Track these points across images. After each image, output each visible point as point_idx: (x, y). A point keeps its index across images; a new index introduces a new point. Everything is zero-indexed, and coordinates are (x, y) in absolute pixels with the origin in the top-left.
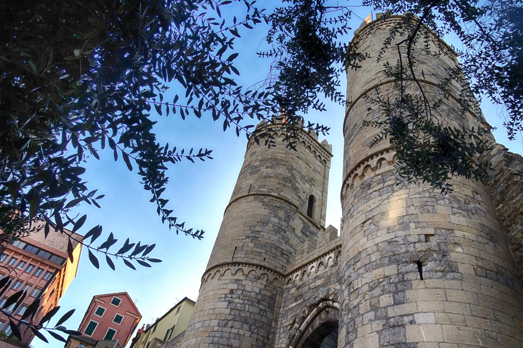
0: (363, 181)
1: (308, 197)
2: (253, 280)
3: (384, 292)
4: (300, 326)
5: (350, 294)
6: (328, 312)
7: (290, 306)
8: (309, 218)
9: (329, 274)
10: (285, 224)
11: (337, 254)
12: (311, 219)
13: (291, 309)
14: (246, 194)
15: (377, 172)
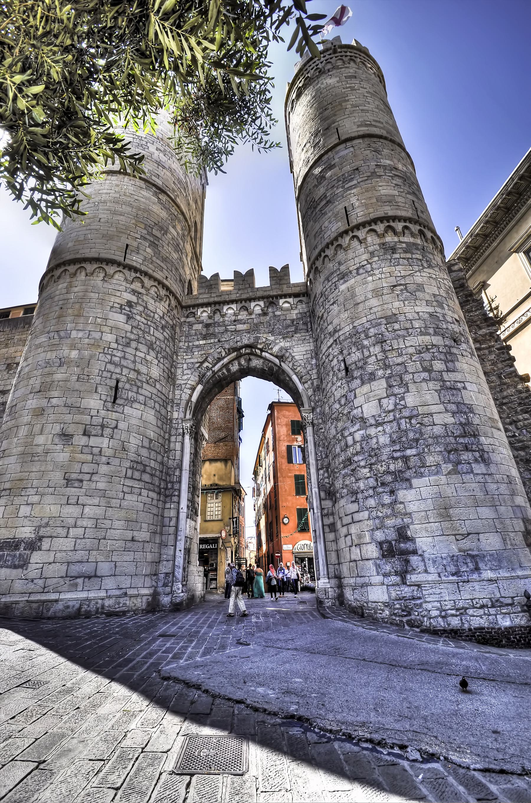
3: (434, 358)
4: (214, 366)
5: (384, 351)
6: (250, 360)
7: (197, 343)
10: (181, 242)
13: (197, 346)
15: (402, 239)
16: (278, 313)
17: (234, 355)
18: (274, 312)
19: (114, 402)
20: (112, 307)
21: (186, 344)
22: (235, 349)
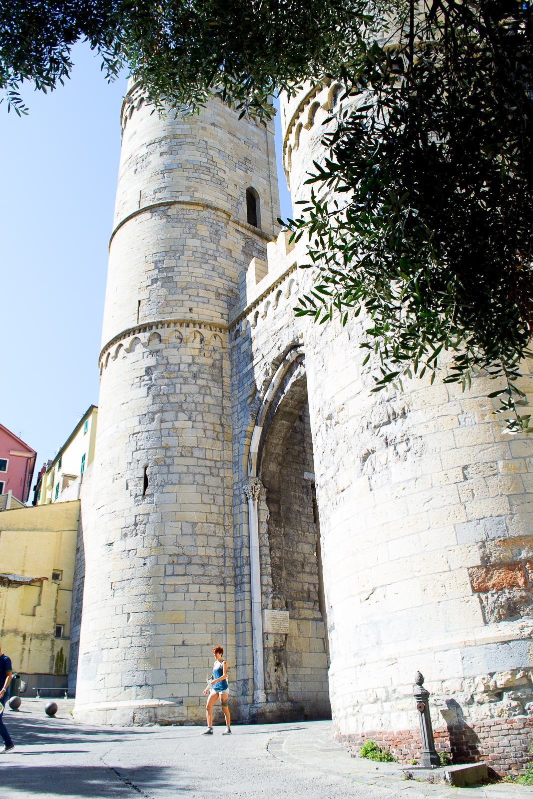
1: (245, 192)
4: (264, 395)
8: (252, 227)
10: (213, 246)
12: (257, 229)
14: (136, 209)
19: (144, 494)
22: (281, 359)
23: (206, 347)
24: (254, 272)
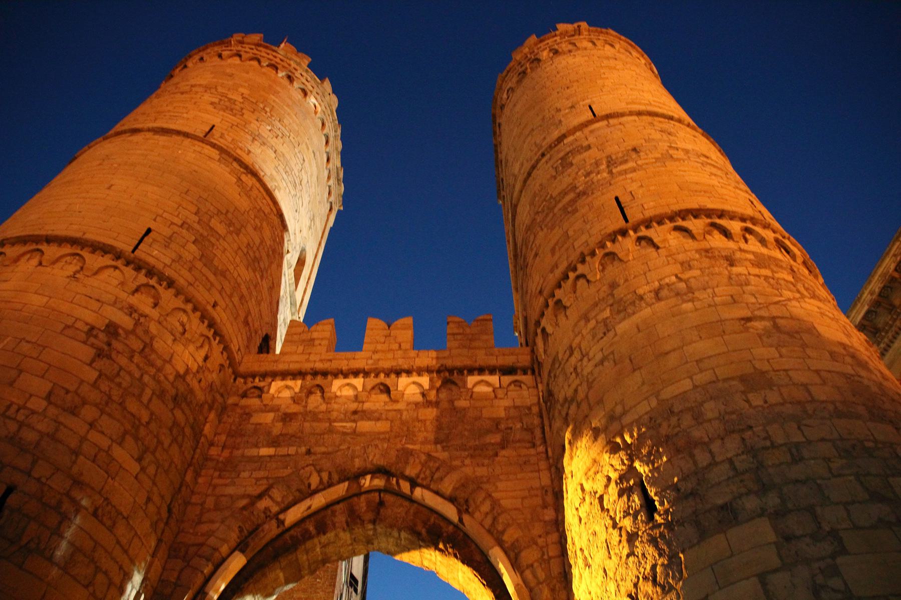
0: (704, 245)
2: (178, 335)
5: (751, 451)
6: (381, 503)
7: (253, 452)
9: (405, 416)
11: (438, 384)
16: (462, 403)
17: (341, 489)
18: (451, 402)
20: (67, 327)
21: (226, 453)
23: (206, 373)
24: (327, 334)
